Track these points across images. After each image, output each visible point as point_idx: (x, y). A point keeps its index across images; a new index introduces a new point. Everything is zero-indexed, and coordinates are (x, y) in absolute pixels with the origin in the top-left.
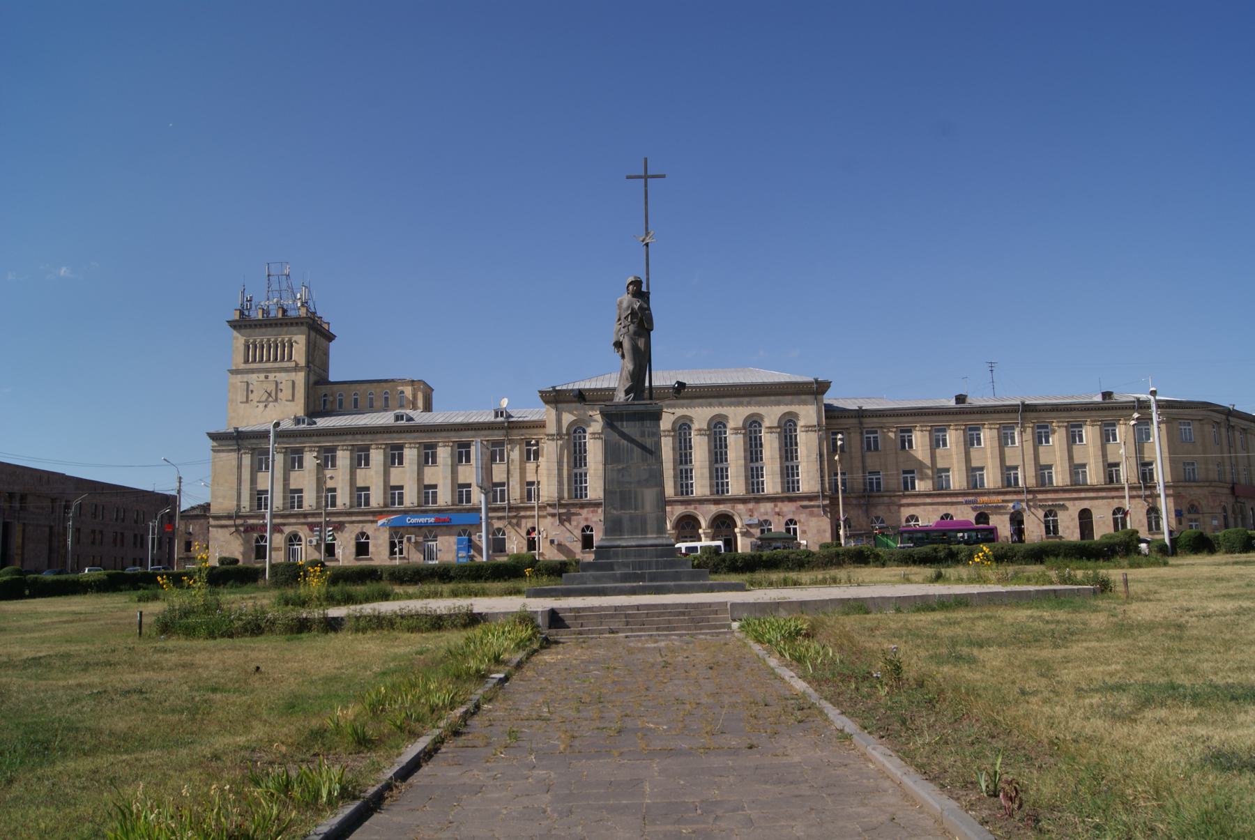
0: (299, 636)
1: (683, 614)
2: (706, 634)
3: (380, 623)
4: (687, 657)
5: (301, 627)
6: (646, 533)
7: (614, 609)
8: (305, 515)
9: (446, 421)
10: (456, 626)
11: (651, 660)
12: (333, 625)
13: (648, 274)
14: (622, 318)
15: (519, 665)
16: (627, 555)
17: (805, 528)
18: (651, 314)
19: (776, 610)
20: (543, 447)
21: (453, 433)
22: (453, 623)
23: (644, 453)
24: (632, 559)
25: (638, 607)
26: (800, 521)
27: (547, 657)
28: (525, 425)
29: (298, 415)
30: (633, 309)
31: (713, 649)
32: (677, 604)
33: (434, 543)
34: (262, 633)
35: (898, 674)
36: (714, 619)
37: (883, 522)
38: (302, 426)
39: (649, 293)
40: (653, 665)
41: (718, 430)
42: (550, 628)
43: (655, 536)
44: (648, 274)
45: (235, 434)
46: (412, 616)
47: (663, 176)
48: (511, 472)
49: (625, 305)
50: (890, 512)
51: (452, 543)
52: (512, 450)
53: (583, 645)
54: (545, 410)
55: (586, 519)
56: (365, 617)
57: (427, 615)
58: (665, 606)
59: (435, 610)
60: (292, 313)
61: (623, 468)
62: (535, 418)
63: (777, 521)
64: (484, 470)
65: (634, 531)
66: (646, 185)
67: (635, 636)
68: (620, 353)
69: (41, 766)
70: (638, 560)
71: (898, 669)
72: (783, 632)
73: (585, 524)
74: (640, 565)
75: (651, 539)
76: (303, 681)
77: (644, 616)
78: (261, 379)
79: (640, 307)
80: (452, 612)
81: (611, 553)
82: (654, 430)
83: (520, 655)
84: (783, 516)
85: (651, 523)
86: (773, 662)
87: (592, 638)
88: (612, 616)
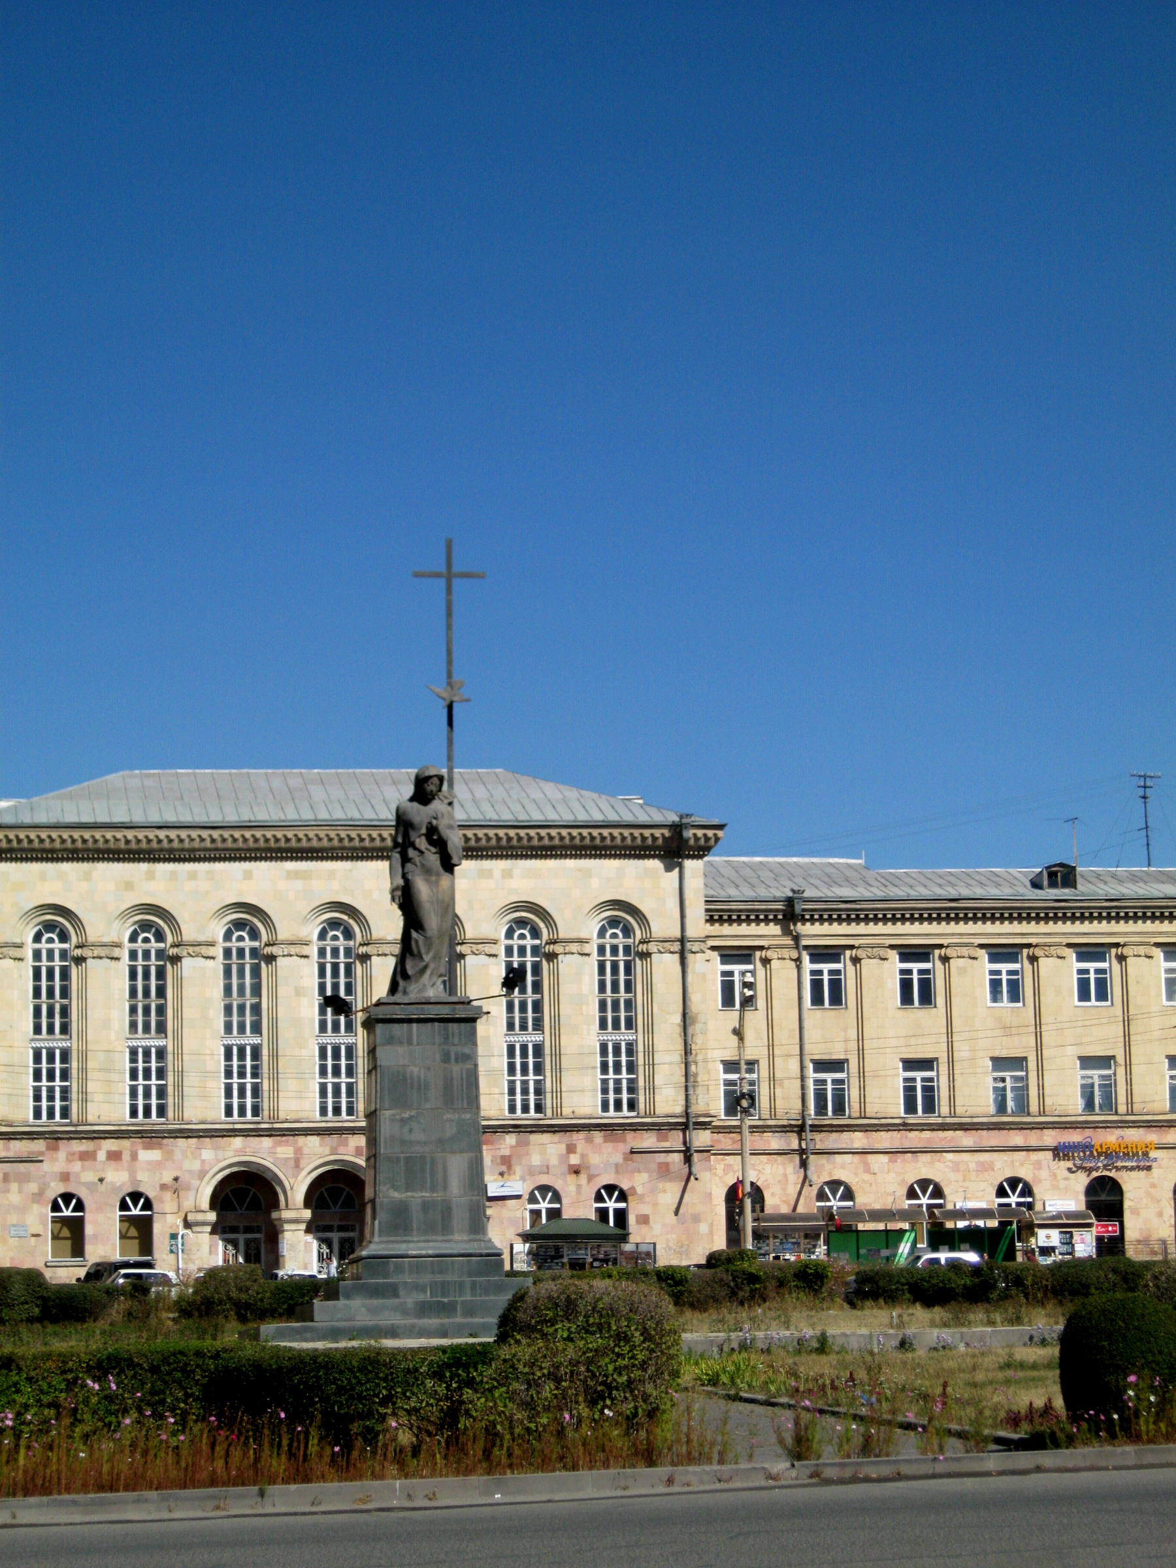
6: (452, 1233)
16: (418, 1269)
17: (645, 1209)
43: (465, 1238)
55: (65, 1177)
61: (411, 1117)
63: (572, 1189)
65: (430, 1229)
70: (439, 1278)
73: (62, 1189)
74: (444, 1288)
75: (459, 1242)
81: (392, 1267)
82: (467, 1050)
85: (460, 1218)
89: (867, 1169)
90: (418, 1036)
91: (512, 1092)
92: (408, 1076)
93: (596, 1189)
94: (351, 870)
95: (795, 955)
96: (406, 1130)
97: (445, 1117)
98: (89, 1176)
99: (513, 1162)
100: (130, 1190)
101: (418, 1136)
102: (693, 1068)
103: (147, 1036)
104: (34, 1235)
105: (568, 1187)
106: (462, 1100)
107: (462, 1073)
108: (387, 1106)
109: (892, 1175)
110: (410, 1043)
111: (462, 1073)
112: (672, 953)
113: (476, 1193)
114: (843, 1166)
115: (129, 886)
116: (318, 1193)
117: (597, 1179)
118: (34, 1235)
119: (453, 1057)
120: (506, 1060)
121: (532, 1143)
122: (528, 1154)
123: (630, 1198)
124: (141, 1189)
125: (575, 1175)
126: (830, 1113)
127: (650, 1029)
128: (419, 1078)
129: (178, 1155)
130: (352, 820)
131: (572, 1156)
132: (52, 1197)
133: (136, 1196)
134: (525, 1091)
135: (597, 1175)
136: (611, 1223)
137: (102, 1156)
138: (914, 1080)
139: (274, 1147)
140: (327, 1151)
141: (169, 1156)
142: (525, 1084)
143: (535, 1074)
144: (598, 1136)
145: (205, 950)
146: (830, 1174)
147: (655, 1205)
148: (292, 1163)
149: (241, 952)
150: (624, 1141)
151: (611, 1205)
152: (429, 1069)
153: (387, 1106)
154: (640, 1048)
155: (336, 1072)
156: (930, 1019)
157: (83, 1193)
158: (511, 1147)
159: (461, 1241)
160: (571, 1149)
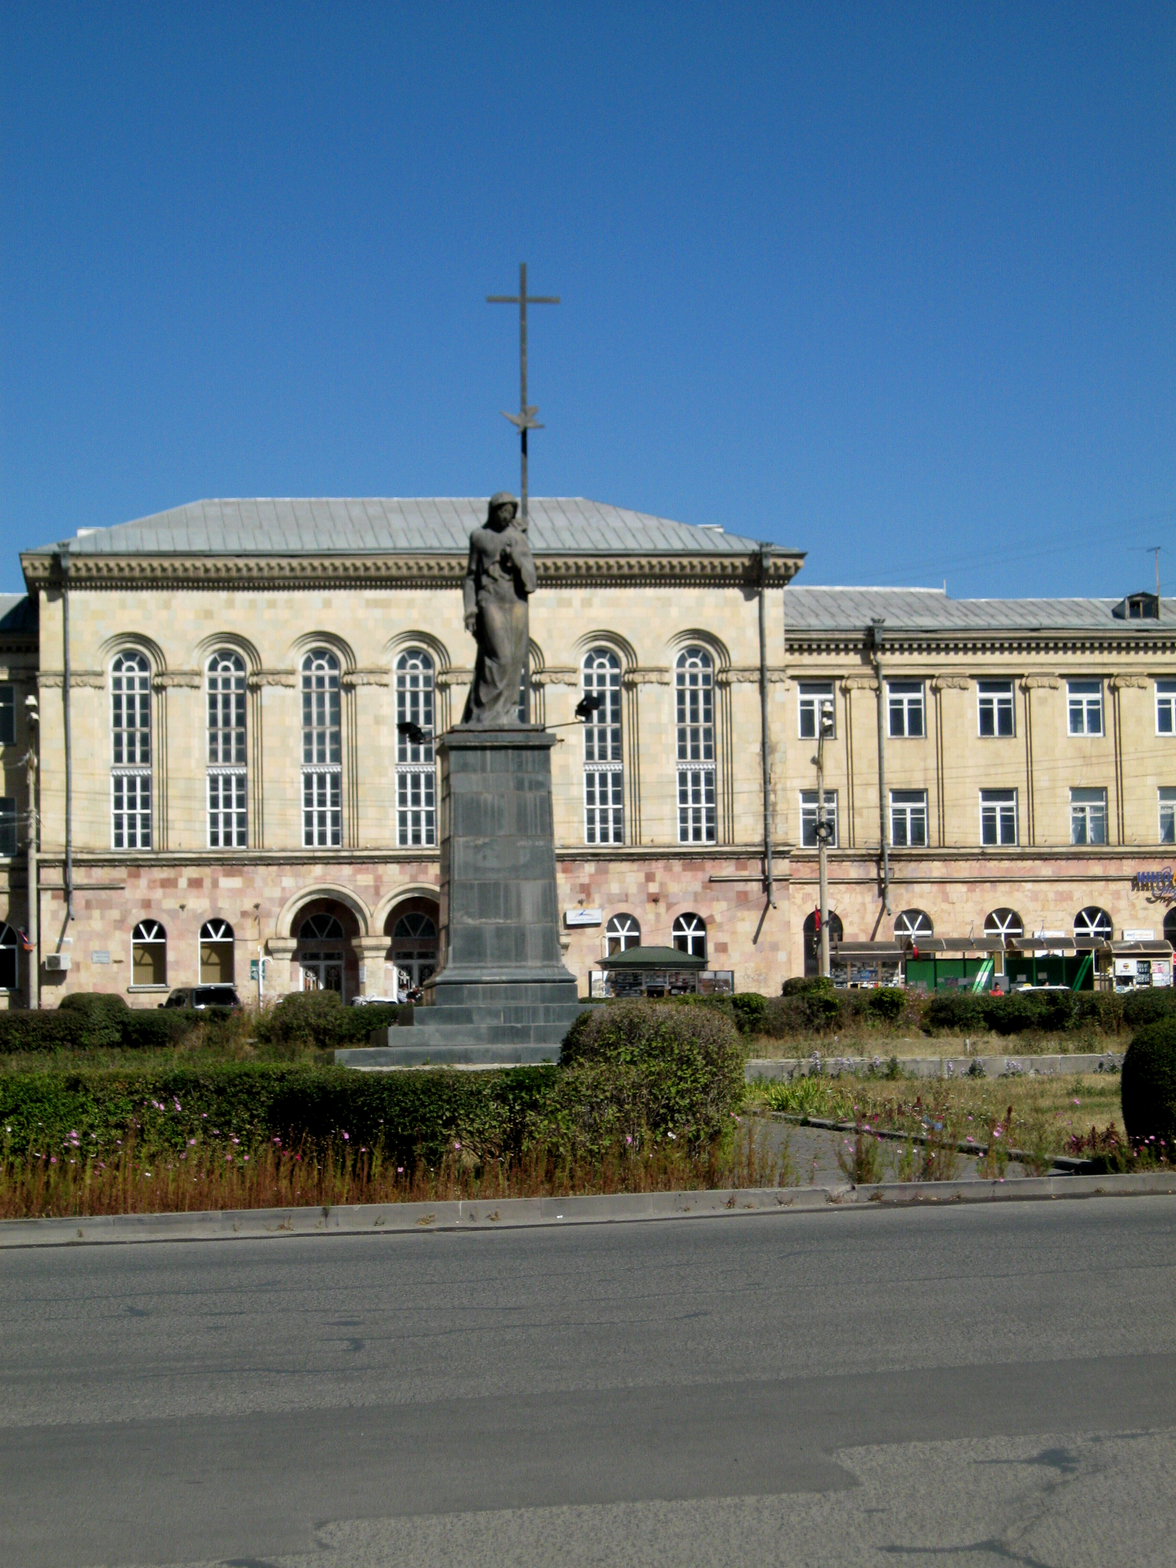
6: (525, 959)
16: (492, 995)
17: (723, 937)
43: (539, 964)
55: (147, 904)
61: (485, 845)
63: (651, 917)
65: (503, 955)
66: (523, 316)
69: (82, 1203)
70: (513, 1004)
73: (144, 916)
74: (518, 1013)
75: (533, 968)
81: (466, 992)
82: (540, 778)
84: (669, 906)
85: (533, 944)
89: (946, 899)
90: (491, 764)
91: (591, 820)
93: (674, 918)
94: (430, 599)
95: (875, 684)
96: (480, 856)
97: (519, 844)
98: (171, 904)
99: (593, 889)
100: (211, 917)
101: (492, 863)
102: (772, 797)
103: (227, 764)
104: (116, 962)
105: (646, 915)
106: (536, 826)
107: (535, 799)
109: (970, 904)
110: (483, 770)
111: (535, 799)
112: (752, 682)
114: (921, 896)
115: (208, 614)
116: (397, 921)
117: (676, 907)
118: (116, 962)
119: (526, 784)
120: (585, 789)
121: (611, 871)
122: (607, 882)
123: (708, 927)
124: (222, 916)
125: (653, 904)
126: (909, 842)
127: (729, 758)
128: (493, 806)
129: (258, 882)
130: (431, 548)
132: (134, 924)
133: (217, 923)
134: (604, 820)
135: (676, 904)
136: (690, 951)
137: (183, 883)
138: (993, 810)
139: (354, 874)
140: (407, 878)
141: (249, 883)
142: (604, 812)
143: (615, 803)
144: (677, 865)
145: (284, 679)
146: (908, 903)
147: (734, 933)
148: (372, 890)
149: (320, 681)
150: (703, 869)
151: (690, 933)
152: (503, 796)
153: (461, 834)
154: (720, 776)
155: (416, 800)
156: (1009, 750)
157: (165, 921)
158: (591, 876)
159: (535, 968)
160: (650, 878)
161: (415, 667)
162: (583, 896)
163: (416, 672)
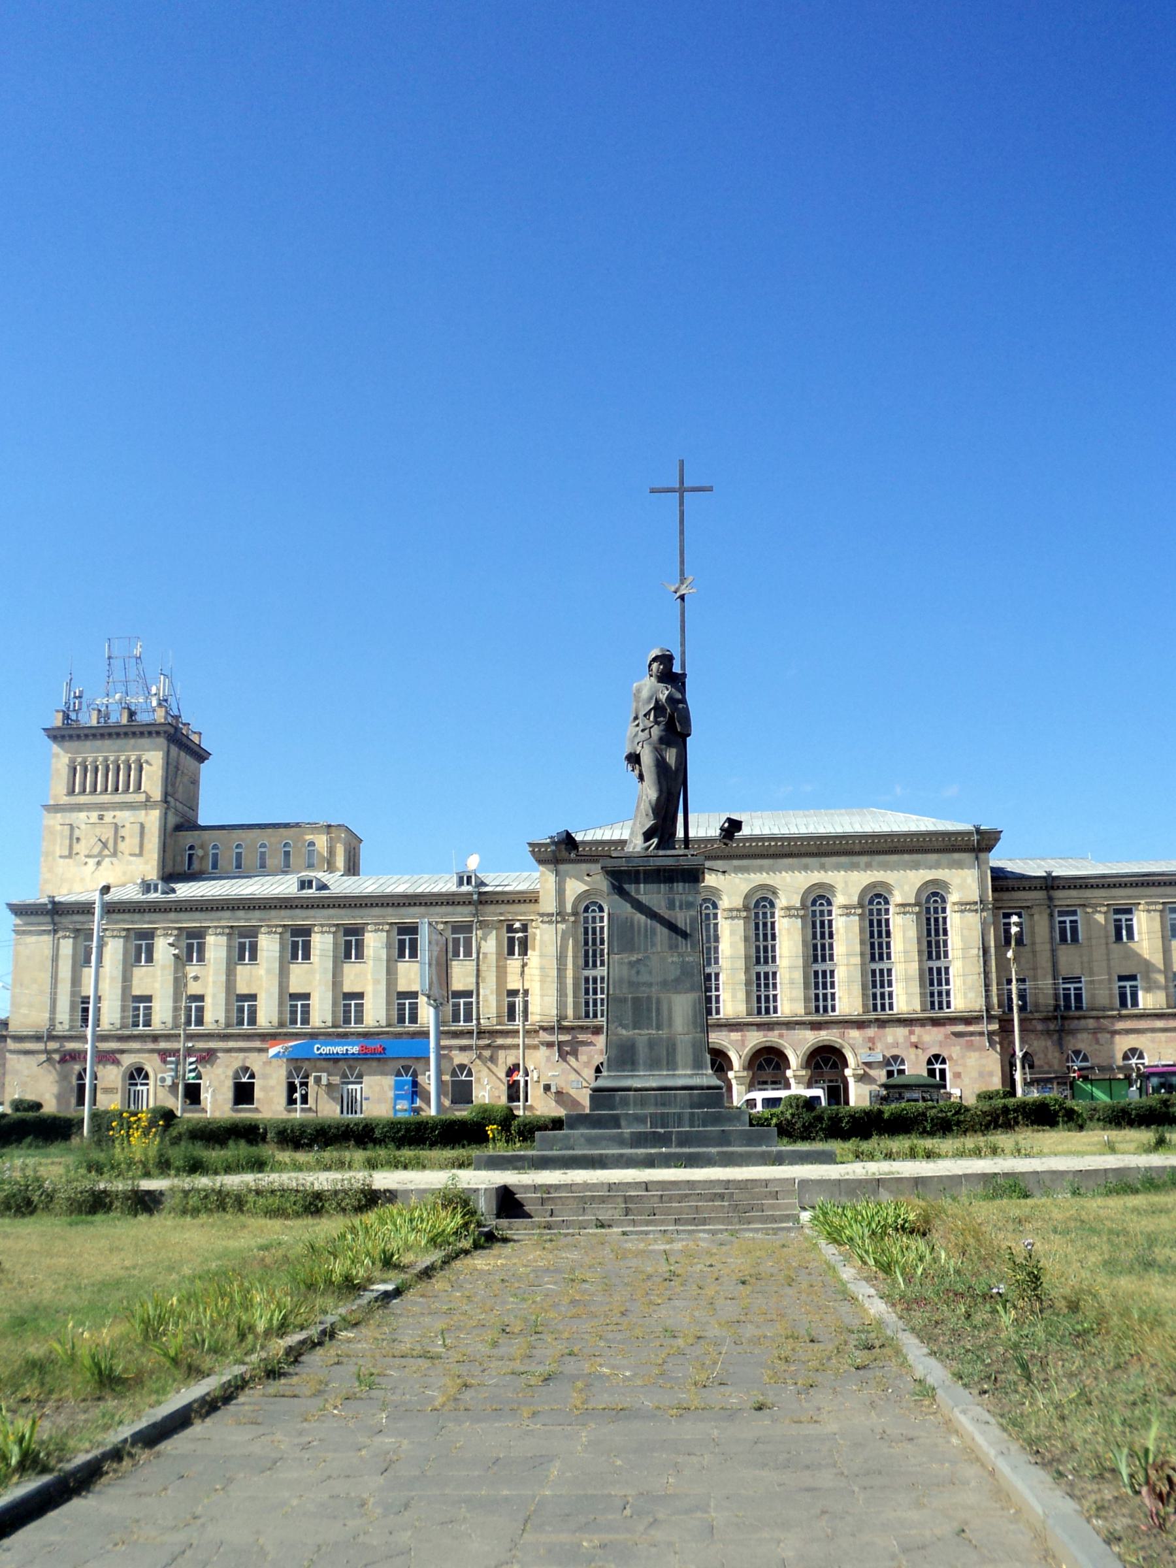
0: (90, 1218)
1: (722, 1197)
2: (756, 1230)
3: (223, 1202)
4: (711, 1266)
5: (97, 1203)
7: (606, 1188)
8: (155, 1038)
9: (380, 890)
10: (344, 1210)
11: (650, 1270)
12: (146, 1203)
13: (683, 644)
14: (641, 715)
15: (427, 1273)
16: (643, 1103)
17: (959, 1069)
18: (687, 710)
19: (875, 1192)
20: (535, 934)
21: (390, 910)
22: (339, 1205)
23: (674, 935)
24: (651, 1110)
25: (647, 1186)
26: (951, 1058)
27: (481, 1261)
28: (505, 898)
29: (148, 878)
30: (657, 701)
31: (758, 1254)
32: (711, 1181)
33: (358, 1087)
34: (32, 1213)
35: (1035, 1289)
36: (773, 1207)
37: (1085, 1059)
38: (152, 896)
39: (684, 675)
40: (649, 1277)
41: (818, 908)
42: (498, 1216)
44: (683, 644)
45: (50, 907)
46: (273, 1192)
47: (710, 489)
48: (483, 974)
49: (645, 694)
50: (1097, 1042)
51: (386, 1088)
52: (484, 938)
53: (548, 1245)
54: (537, 874)
56: (198, 1191)
57: (297, 1191)
58: (691, 1184)
59: (312, 1184)
60: (142, 718)
61: (639, 961)
62: (522, 887)
63: (913, 1057)
64: (434, 967)
65: (654, 1064)
66: (682, 504)
67: (637, 1233)
68: (637, 772)
71: (1035, 1279)
72: (874, 1226)
74: (663, 1120)
76: (66, 1287)
77: (656, 1199)
78: (92, 821)
79: (670, 698)
80: (339, 1187)
81: (618, 1099)
82: (691, 899)
83: (436, 1256)
86: (847, 1273)
87: (566, 1235)
88: (603, 1200)
92: (636, 923)
96: (633, 972)
107: (686, 920)
108: (616, 950)
111: (686, 920)
113: (699, 1030)
114: (1083, 1041)
119: (677, 904)
131: (912, 1036)
136: (938, 1078)
147: (964, 1065)
148: (740, 1043)
153: (616, 950)
161: (764, 906)
162: (870, 1045)
163: (766, 910)
